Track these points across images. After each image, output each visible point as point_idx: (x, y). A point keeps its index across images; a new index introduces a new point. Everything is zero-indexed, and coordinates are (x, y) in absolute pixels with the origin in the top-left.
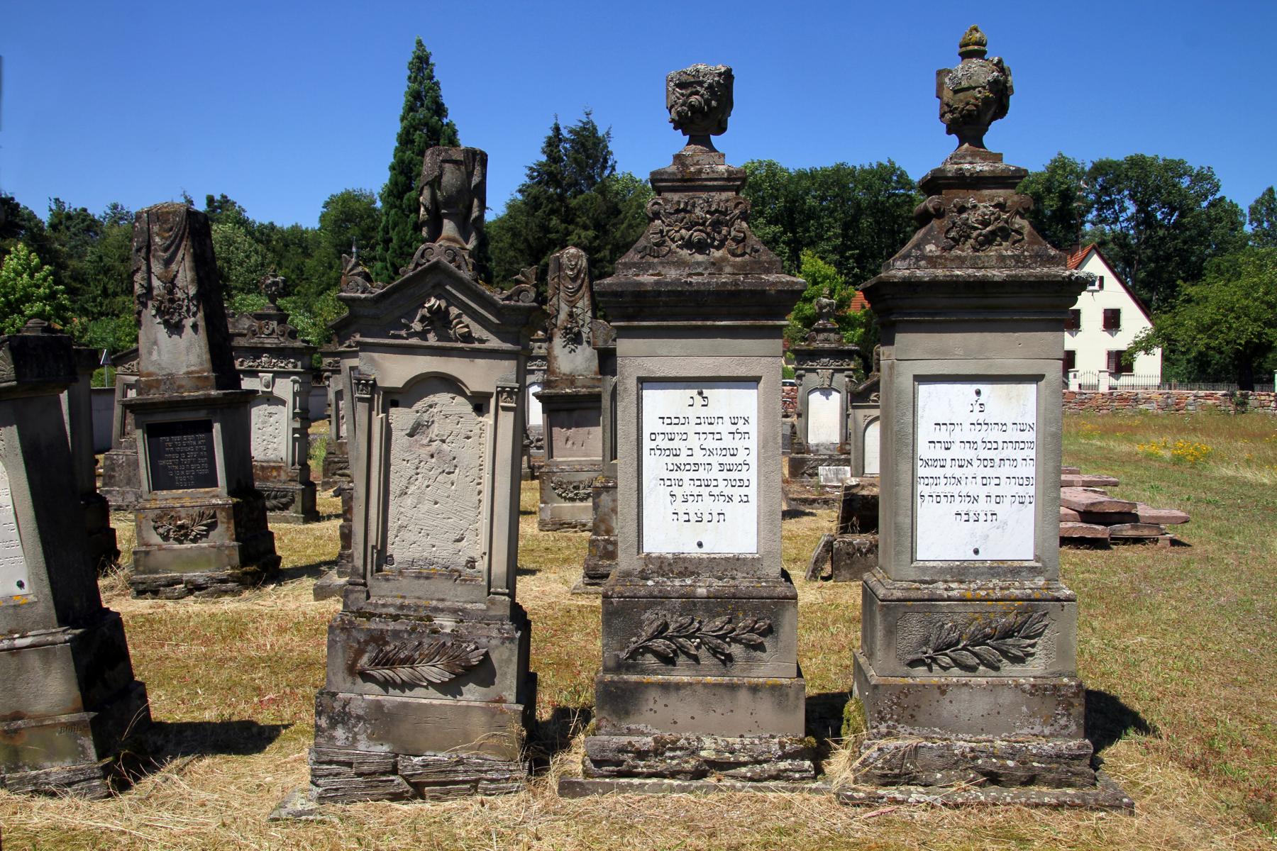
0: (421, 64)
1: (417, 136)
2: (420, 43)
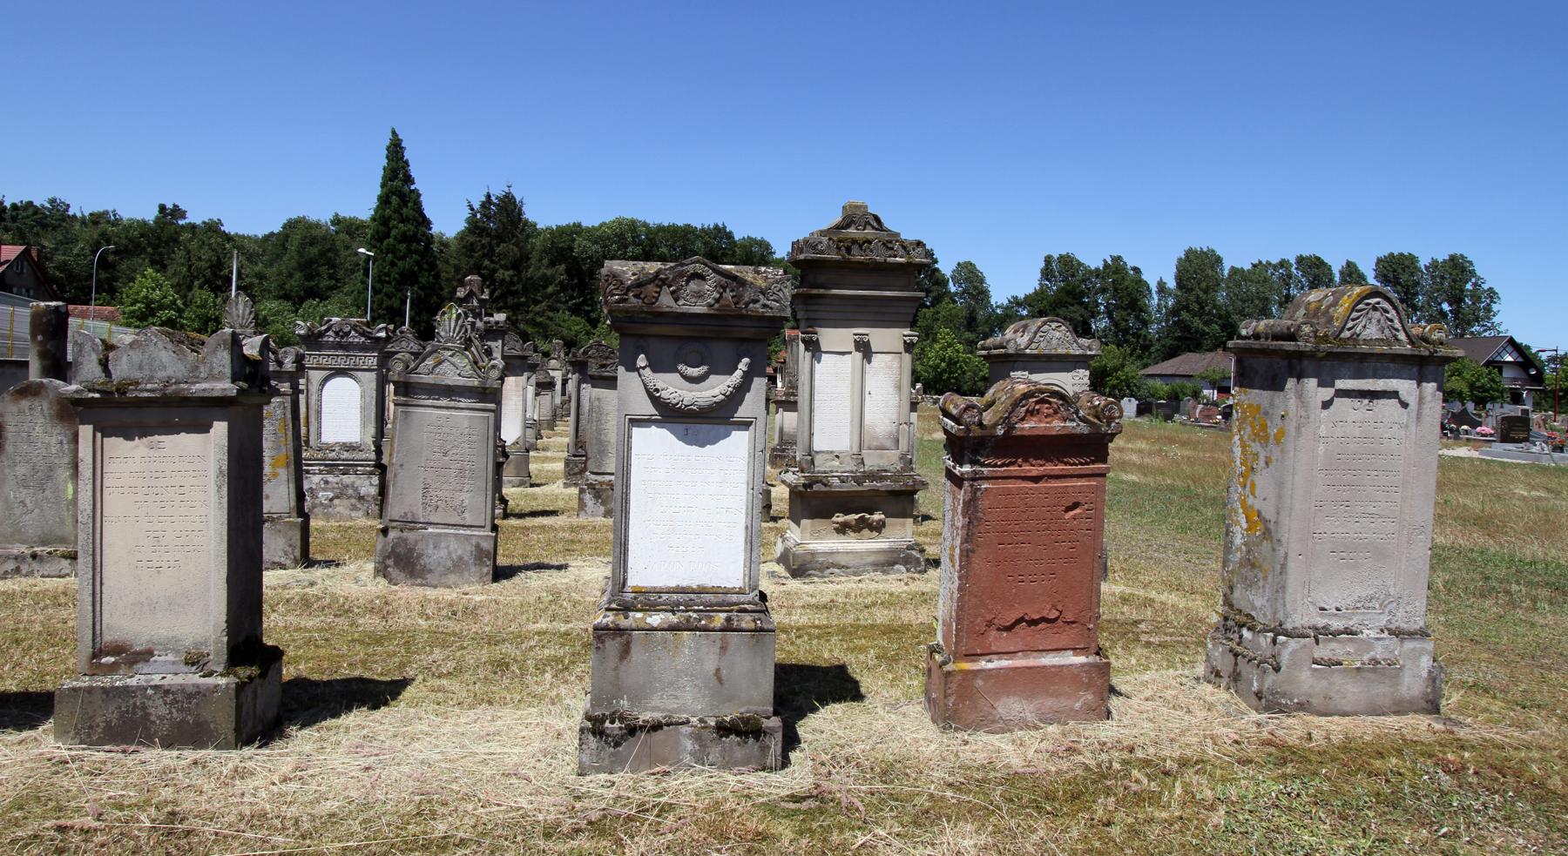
0: (396, 150)
1: (395, 200)
2: (394, 133)
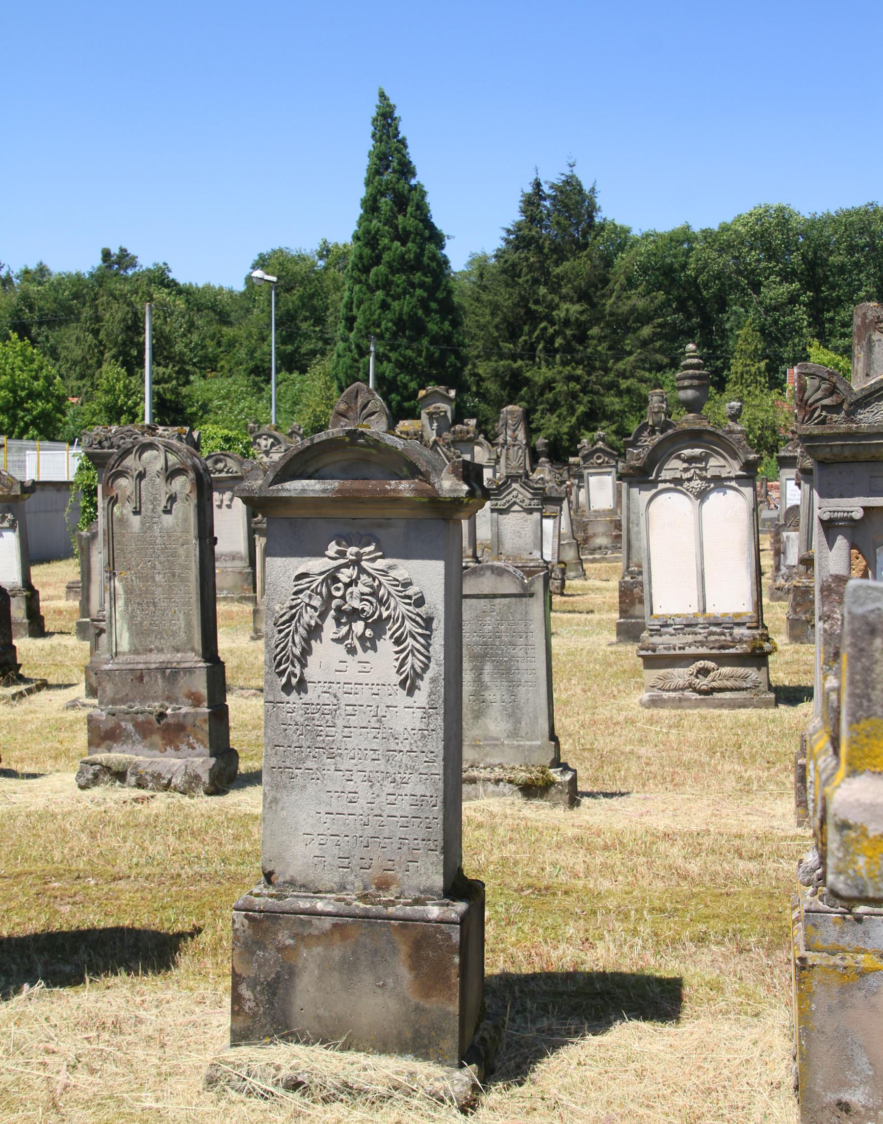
0: (386, 122)
